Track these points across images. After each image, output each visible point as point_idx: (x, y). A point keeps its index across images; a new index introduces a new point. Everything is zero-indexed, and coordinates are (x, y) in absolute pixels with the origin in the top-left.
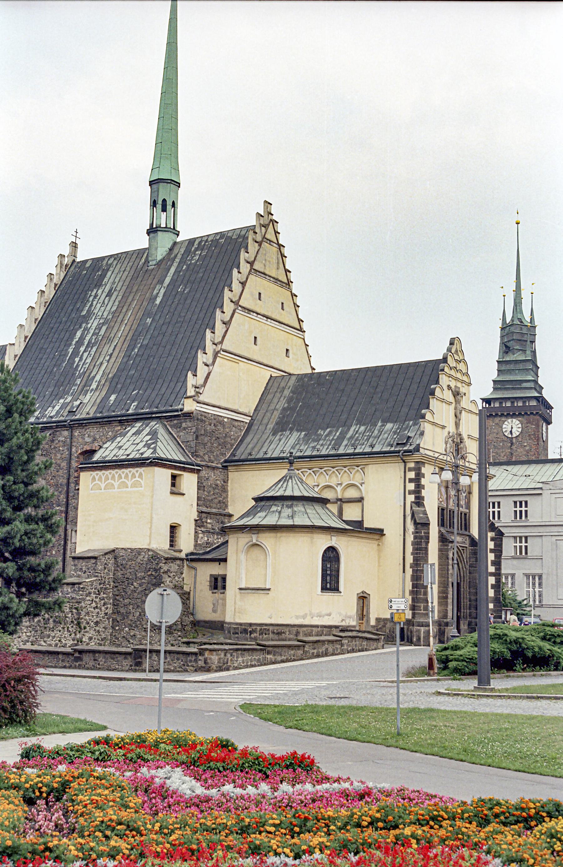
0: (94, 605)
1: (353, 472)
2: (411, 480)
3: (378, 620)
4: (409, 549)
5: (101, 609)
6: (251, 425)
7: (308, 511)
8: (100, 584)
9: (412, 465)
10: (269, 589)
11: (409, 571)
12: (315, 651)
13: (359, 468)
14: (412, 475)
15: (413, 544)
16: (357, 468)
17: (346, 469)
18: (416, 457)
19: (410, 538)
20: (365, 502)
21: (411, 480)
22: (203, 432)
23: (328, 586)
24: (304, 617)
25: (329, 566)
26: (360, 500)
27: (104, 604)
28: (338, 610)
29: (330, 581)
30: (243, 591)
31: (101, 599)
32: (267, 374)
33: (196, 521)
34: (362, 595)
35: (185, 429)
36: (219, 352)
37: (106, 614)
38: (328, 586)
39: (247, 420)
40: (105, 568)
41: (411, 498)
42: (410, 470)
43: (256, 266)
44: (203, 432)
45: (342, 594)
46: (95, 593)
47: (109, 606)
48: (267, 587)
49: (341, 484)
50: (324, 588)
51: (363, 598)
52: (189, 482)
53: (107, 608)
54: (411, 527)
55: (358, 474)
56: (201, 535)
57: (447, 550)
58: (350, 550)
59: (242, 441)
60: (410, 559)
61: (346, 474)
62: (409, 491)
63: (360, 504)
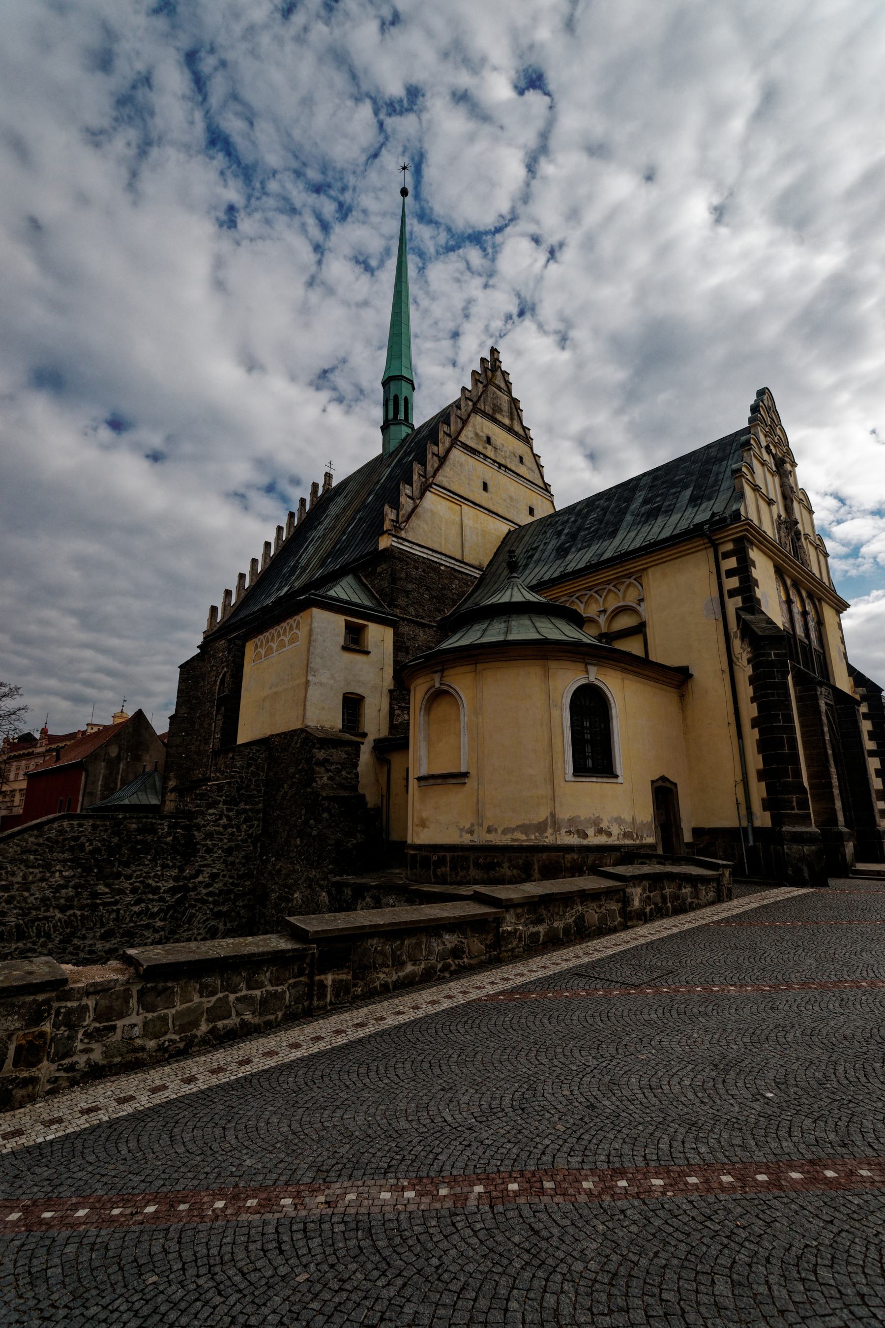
0: (224, 821)
1: (622, 588)
2: (730, 573)
3: (696, 831)
4: (746, 691)
5: (239, 830)
6: (482, 578)
7: (538, 624)
9: (730, 546)
10: (466, 775)
11: (752, 735)
12: (541, 929)
13: (632, 580)
14: (731, 563)
15: (752, 680)
16: (628, 581)
17: (611, 587)
18: (735, 531)
19: (744, 671)
20: (649, 631)
21: (730, 573)
22: (403, 575)
23: (590, 763)
24: (541, 827)
26: (640, 629)
27: (245, 821)
28: (616, 809)
29: (593, 753)
30: (422, 783)
31: (239, 813)
32: (504, 528)
33: (390, 691)
34: (660, 783)
35: (380, 574)
36: (430, 485)
37: (250, 836)
38: (590, 763)
39: (477, 574)
40: (249, 765)
41: (734, 604)
42: (726, 555)
43: (481, 406)
44: (403, 575)
45: (620, 780)
47: (256, 823)
48: (463, 770)
49: (604, 611)
50: (580, 769)
51: (664, 794)
52: (380, 637)
53: (251, 827)
54: (742, 652)
55: (631, 590)
56: (397, 712)
57: (816, 698)
58: (631, 705)
59: (468, 598)
60: (750, 711)
61: (611, 595)
62: (729, 591)
63: (640, 637)
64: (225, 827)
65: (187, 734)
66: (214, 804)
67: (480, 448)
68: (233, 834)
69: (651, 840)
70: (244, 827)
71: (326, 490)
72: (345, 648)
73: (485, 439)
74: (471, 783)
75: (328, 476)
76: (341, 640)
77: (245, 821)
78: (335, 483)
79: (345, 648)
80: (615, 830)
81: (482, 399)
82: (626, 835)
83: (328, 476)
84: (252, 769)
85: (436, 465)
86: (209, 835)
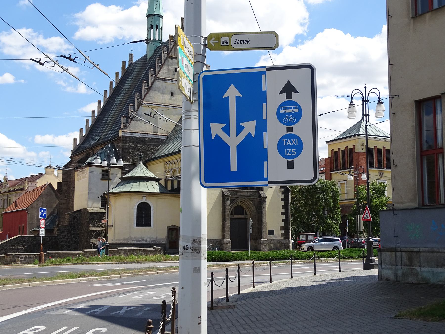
0: (67, 237)
5: (72, 239)
8: (71, 227)
23: (144, 223)
24: (127, 239)
25: (144, 212)
27: (74, 237)
31: (71, 235)
37: (76, 242)
38: (144, 223)
40: (74, 219)
46: (67, 231)
50: (138, 225)
64: (67, 239)
65: (68, 198)
66: (64, 232)
67: (171, 77)
68: (70, 241)
69: (164, 243)
70: (74, 239)
71: (130, 65)
72: (101, 179)
73: (174, 70)
74: (113, 228)
75: (131, 55)
76: (100, 176)
77: (74, 237)
78: (135, 60)
79: (101, 179)
80: (148, 240)
81: (173, 49)
82: (152, 241)
83: (131, 55)
84: (75, 220)
85: (145, 92)
86: (62, 241)
